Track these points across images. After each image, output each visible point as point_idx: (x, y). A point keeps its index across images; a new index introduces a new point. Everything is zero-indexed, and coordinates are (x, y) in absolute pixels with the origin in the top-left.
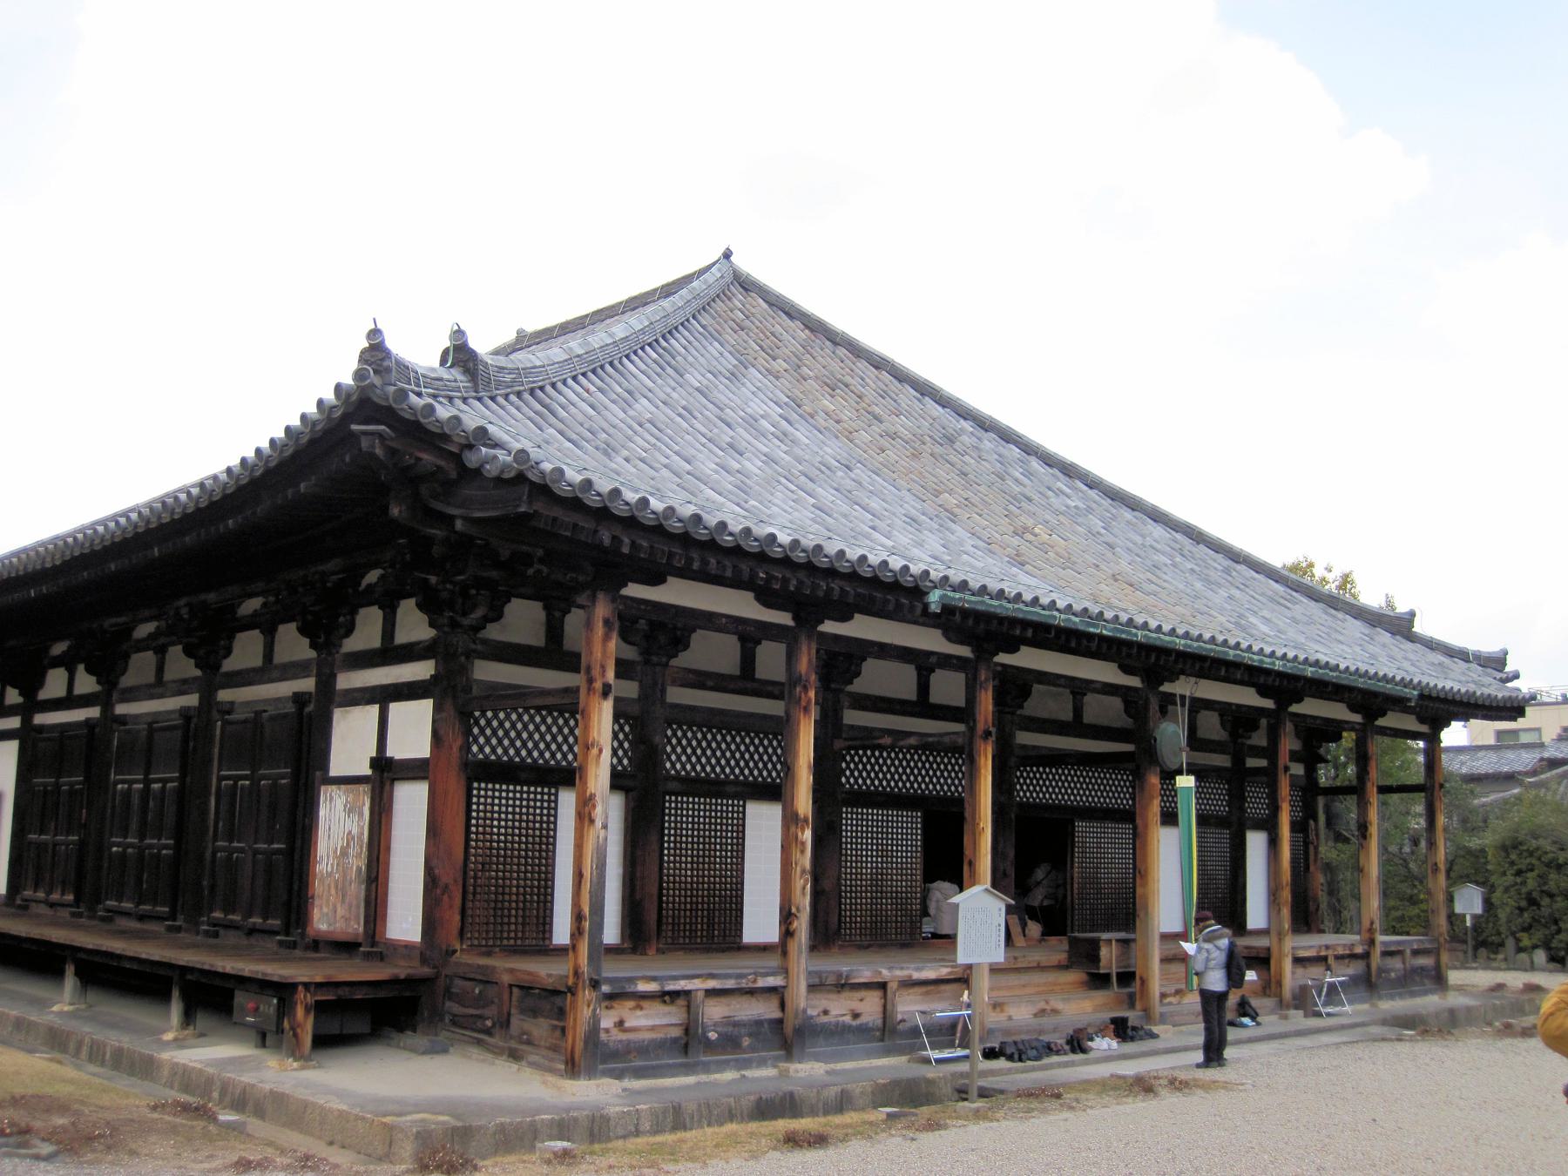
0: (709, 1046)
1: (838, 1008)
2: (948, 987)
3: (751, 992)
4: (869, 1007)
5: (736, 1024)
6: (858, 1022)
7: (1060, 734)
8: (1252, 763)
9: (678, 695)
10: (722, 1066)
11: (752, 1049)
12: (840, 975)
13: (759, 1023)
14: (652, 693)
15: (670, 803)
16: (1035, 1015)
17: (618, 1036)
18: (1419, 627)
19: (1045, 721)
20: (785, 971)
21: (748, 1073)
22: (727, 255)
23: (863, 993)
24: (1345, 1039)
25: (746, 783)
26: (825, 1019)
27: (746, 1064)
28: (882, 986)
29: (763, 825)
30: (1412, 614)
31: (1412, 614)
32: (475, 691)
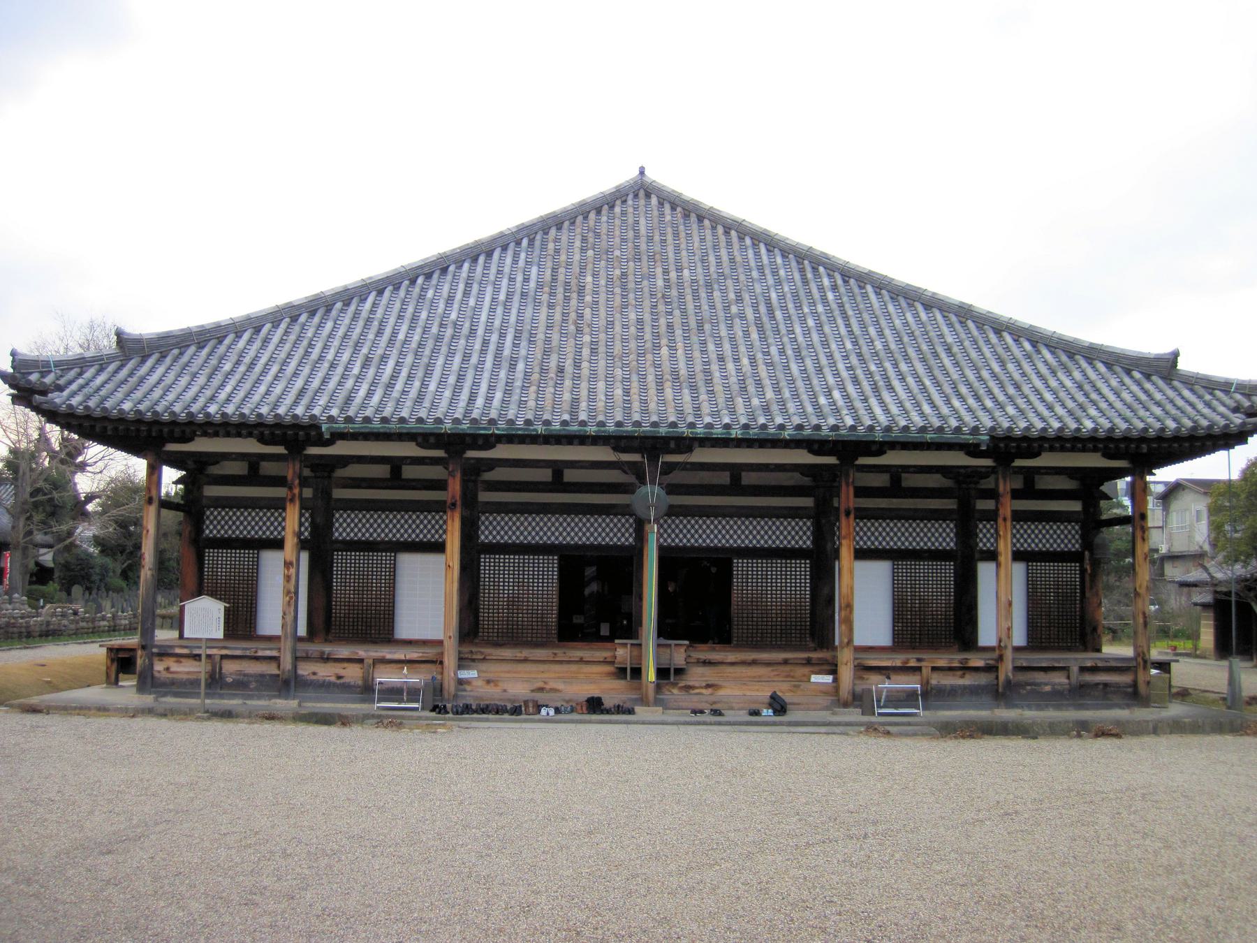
0: (230, 686)
1: (325, 672)
2: (423, 666)
3: (257, 658)
4: (353, 674)
5: (245, 675)
6: (342, 681)
7: (544, 504)
8: (984, 505)
9: (338, 493)
10: (234, 696)
11: (257, 689)
12: (323, 653)
13: (262, 676)
14: (326, 494)
15: (338, 556)
16: (533, 691)
17: (165, 675)
18: (1185, 365)
19: (701, 486)
20: (279, 650)
21: (249, 702)
22: (642, 172)
23: (346, 665)
24: (675, 719)
25: (398, 542)
26: (314, 677)
27: (250, 697)
28: (361, 661)
29: (272, 567)
30: (1176, 355)
31: (1176, 355)
32: (204, 502)
